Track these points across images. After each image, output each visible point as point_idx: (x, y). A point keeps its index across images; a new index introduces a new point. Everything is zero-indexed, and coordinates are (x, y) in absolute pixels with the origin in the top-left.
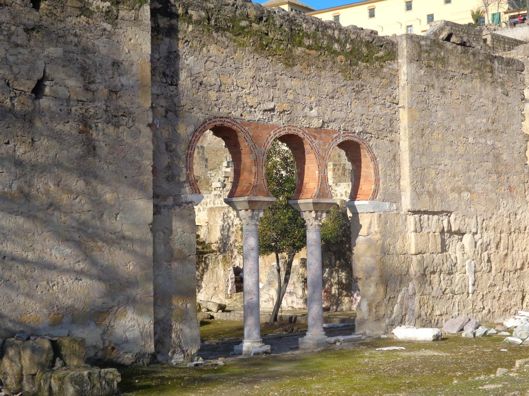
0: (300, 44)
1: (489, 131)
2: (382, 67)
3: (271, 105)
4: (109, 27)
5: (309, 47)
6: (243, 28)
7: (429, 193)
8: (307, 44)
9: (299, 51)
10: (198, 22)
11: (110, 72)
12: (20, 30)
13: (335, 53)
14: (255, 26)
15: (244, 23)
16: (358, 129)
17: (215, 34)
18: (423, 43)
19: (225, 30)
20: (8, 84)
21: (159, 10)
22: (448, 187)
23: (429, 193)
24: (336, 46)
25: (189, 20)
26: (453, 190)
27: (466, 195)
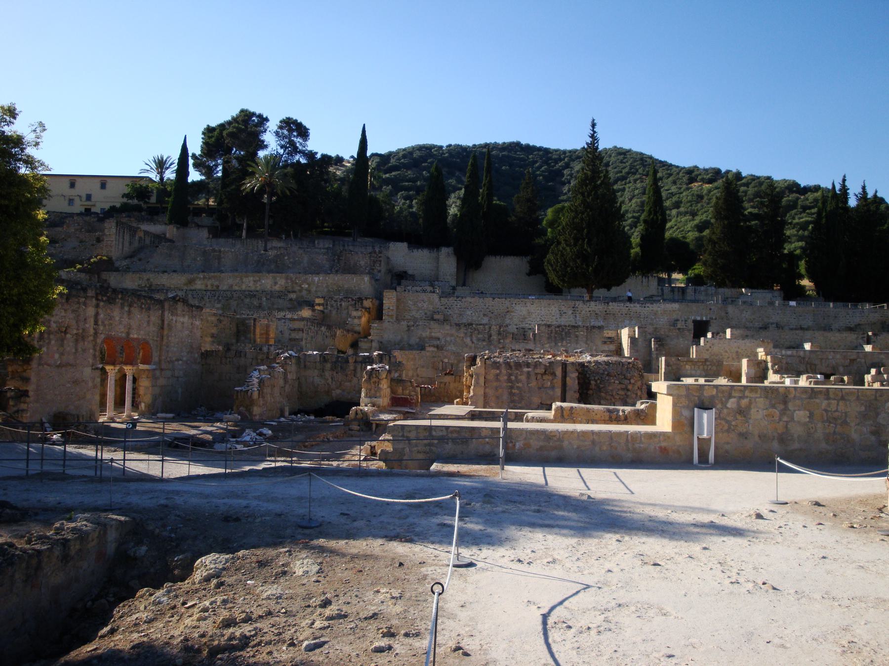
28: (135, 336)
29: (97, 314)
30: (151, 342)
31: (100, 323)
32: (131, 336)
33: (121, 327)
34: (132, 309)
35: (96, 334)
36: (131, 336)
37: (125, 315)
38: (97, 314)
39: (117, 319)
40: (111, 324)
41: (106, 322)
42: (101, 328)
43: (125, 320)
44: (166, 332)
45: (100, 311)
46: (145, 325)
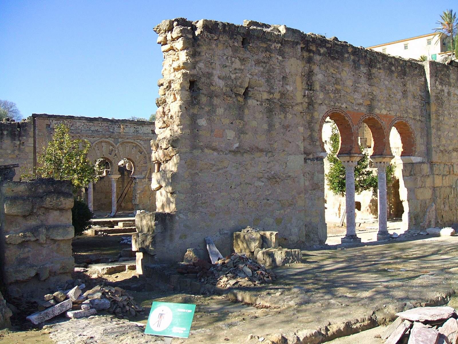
0: (375, 67)
3: (361, 101)
4: (280, 58)
7: (442, 151)
8: (378, 66)
10: (324, 55)
11: (281, 83)
12: (237, 60)
16: (406, 115)
19: (337, 59)
20: (232, 90)
21: (304, 48)
25: (320, 54)
28: (384, 112)
29: (309, 75)
30: (411, 122)
31: (317, 87)
32: (377, 111)
33: (356, 96)
34: (374, 71)
35: (311, 104)
36: (377, 111)
37: (363, 80)
38: (309, 75)
39: (349, 83)
40: (337, 91)
41: (330, 87)
42: (321, 96)
43: (364, 86)
44: (433, 108)
45: (316, 69)
46: (399, 95)
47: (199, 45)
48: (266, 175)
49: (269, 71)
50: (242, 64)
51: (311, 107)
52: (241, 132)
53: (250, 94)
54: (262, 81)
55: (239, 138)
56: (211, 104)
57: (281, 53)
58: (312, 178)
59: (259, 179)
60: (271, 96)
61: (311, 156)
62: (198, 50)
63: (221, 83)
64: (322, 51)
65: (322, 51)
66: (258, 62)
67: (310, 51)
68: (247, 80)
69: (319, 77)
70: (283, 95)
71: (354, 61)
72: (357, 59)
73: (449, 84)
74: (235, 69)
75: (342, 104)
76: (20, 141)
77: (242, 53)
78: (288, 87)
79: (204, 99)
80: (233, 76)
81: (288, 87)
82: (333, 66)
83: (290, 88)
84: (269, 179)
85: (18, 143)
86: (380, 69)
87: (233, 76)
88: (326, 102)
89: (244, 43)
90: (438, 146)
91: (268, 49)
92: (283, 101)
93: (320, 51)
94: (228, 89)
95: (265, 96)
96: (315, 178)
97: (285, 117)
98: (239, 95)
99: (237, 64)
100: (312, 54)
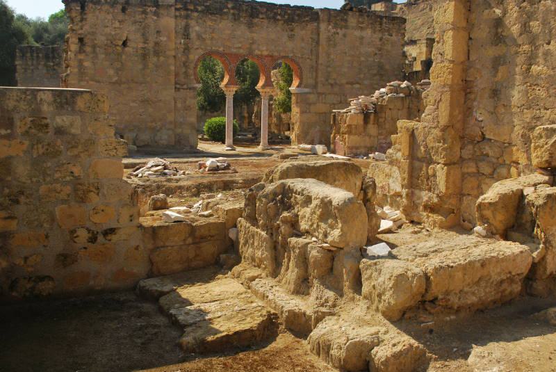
0: (257, 17)
1: (376, 54)
2: (307, 25)
4: (155, 18)
5: (262, 18)
6: (225, 12)
7: (332, 85)
9: (256, 20)
10: (202, 12)
13: (278, 20)
14: (232, 11)
15: (225, 10)
17: (210, 16)
18: (332, 12)
22: (344, 81)
23: (332, 85)
24: (279, 17)
26: (347, 83)
27: (357, 86)
31: (193, 35)
45: (192, 23)
47: (85, 14)
48: (140, 99)
49: (144, 28)
50: (120, 25)
51: (186, 51)
52: (117, 70)
53: (128, 44)
54: (139, 35)
55: (118, 74)
56: (94, 52)
57: (156, 14)
58: (185, 102)
59: (134, 101)
60: (146, 45)
61: (185, 87)
62: (85, 17)
63: (103, 38)
64: (200, 9)
65: (200, 9)
66: (135, 22)
67: (187, 9)
68: (125, 35)
69: (196, 28)
70: (157, 44)
71: (233, 14)
72: (236, 12)
73: (346, 27)
74: (115, 28)
75: (219, 47)
76: (54, 62)
77: (121, 17)
78: (161, 38)
79: (88, 49)
80: (113, 33)
81: (161, 38)
82: (211, 20)
83: (164, 39)
84: (142, 101)
85: (52, 64)
86: (262, 18)
87: (113, 33)
88: (203, 47)
89: (124, 10)
90: (327, 80)
91: (144, 12)
92: (157, 48)
93: (197, 9)
94: (109, 42)
95: (141, 45)
96: (187, 102)
97: (158, 60)
98: (118, 45)
99: (117, 24)
100: (189, 12)
